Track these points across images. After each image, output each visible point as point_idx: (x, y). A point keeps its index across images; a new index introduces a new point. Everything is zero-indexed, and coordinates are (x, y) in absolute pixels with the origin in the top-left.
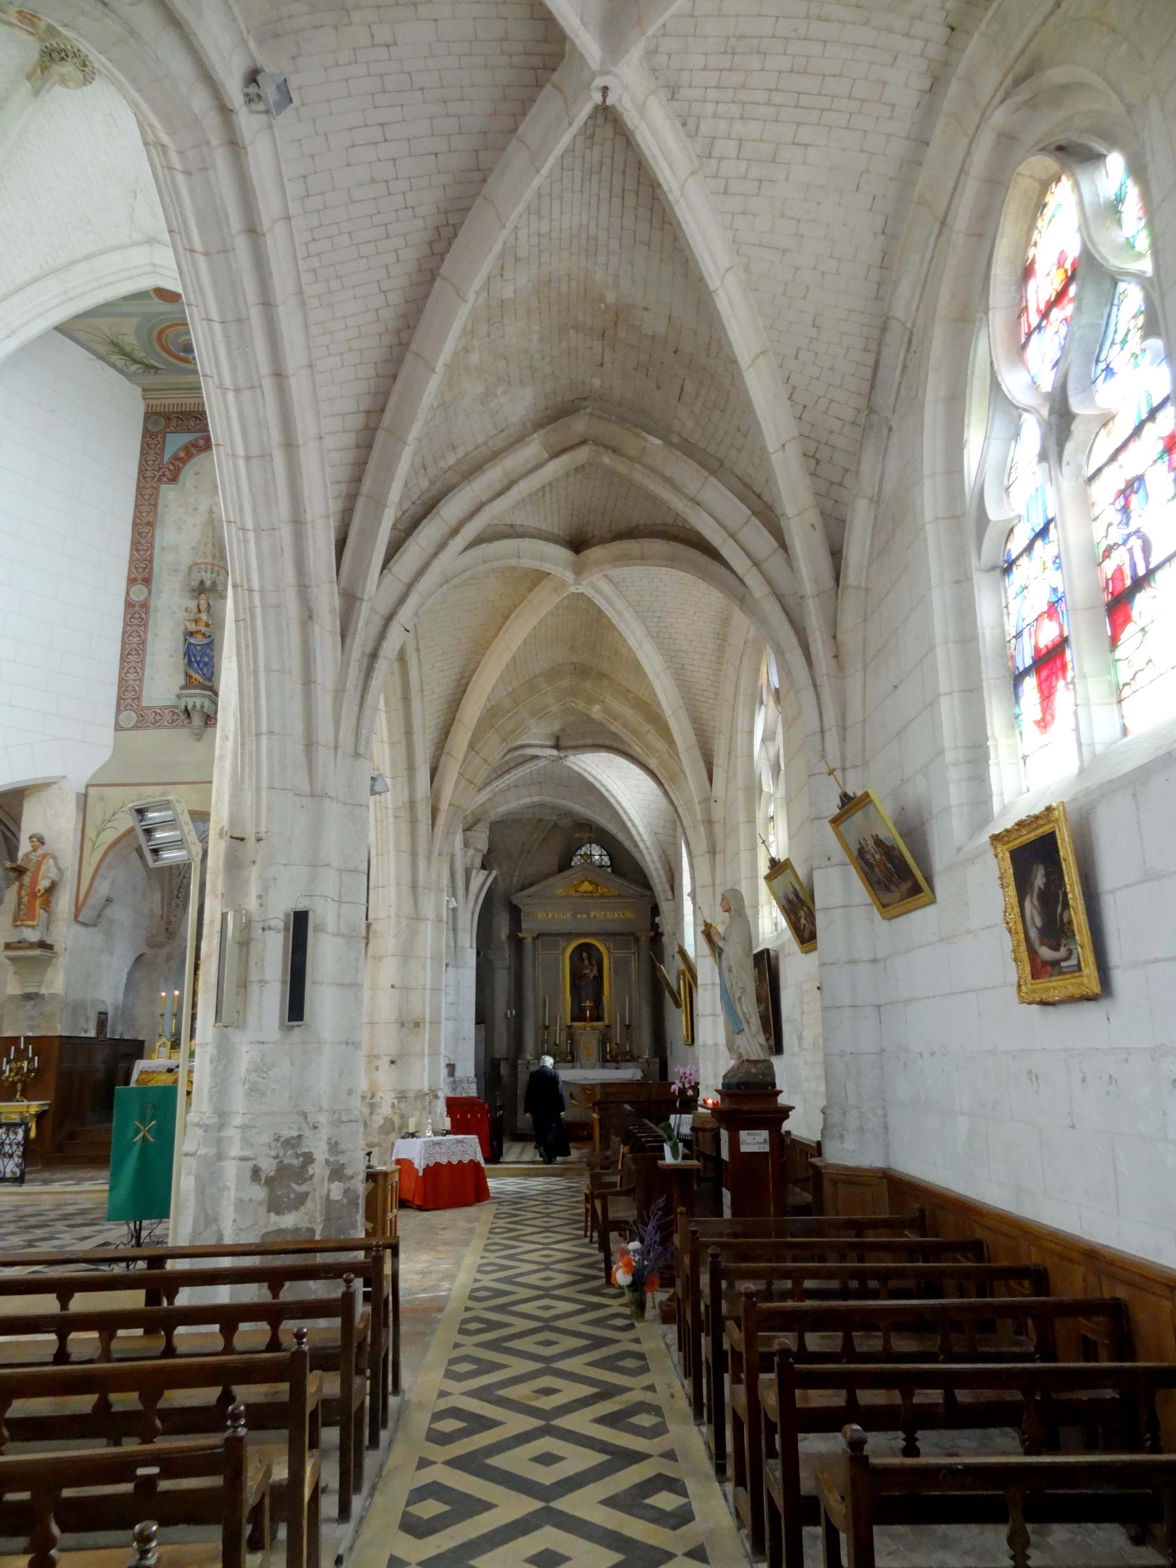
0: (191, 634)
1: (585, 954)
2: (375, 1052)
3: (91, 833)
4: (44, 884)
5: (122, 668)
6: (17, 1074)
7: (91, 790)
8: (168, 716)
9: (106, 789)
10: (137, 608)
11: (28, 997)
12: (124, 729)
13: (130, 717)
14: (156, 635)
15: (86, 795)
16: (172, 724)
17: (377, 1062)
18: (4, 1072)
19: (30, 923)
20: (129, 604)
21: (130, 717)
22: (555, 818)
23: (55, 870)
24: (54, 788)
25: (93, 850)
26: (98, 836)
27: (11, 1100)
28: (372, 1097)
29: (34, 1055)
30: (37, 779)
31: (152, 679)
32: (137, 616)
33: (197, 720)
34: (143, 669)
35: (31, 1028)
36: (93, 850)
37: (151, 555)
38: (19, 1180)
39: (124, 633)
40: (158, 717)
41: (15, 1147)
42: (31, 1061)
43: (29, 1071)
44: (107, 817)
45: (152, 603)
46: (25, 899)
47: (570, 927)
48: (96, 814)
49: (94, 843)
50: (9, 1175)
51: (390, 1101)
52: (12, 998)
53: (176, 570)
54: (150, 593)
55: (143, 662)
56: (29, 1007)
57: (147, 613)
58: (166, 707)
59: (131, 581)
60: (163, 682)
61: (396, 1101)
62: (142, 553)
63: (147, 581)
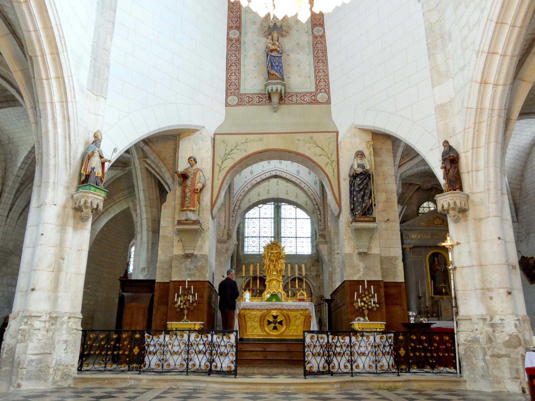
0: (272, 51)
1: (436, 259)
2: (488, 286)
3: (218, 161)
4: (199, 186)
5: (227, 73)
6: (185, 304)
7: (217, 136)
8: (256, 99)
9: (225, 136)
10: (234, 42)
11: (187, 256)
12: (231, 106)
13: (233, 99)
14: (246, 56)
15: (214, 139)
16: (259, 103)
17: (490, 294)
18: (177, 302)
19: (192, 209)
20: (229, 40)
21: (233, 99)
22: (421, 184)
23: (203, 178)
24: (197, 134)
25: (220, 171)
26: (222, 162)
27: (180, 321)
28: (491, 320)
29: (194, 292)
30: (190, 125)
31: (245, 79)
32: (234, 46)
33: (275, 99)
34: (239, 73)
35: (190, 276)
36: (220, 171)
37: (240, 15)
38: (233, 373)
39: (227, 54)
40: (250, 100)
41: (229, 349)
42: (194, 295)
43: (193, 302)
44: (227, 152)
45: (242, 39)
46: (188, 195)
47: (431, 243)
48: (221, 151)
49: (220, 167)
50: (225, 369)
51: (513, 323)
52: (177, 256)
53: (255, 22)
54: (240, 33)
55: (239, 70)
56: (188, 263)
57: (240, 44)
58: (255, 94)
59: (230, 28)
60: (252, 81)
61: (517, 322)
62: (235, 13)
63: (239, 28)
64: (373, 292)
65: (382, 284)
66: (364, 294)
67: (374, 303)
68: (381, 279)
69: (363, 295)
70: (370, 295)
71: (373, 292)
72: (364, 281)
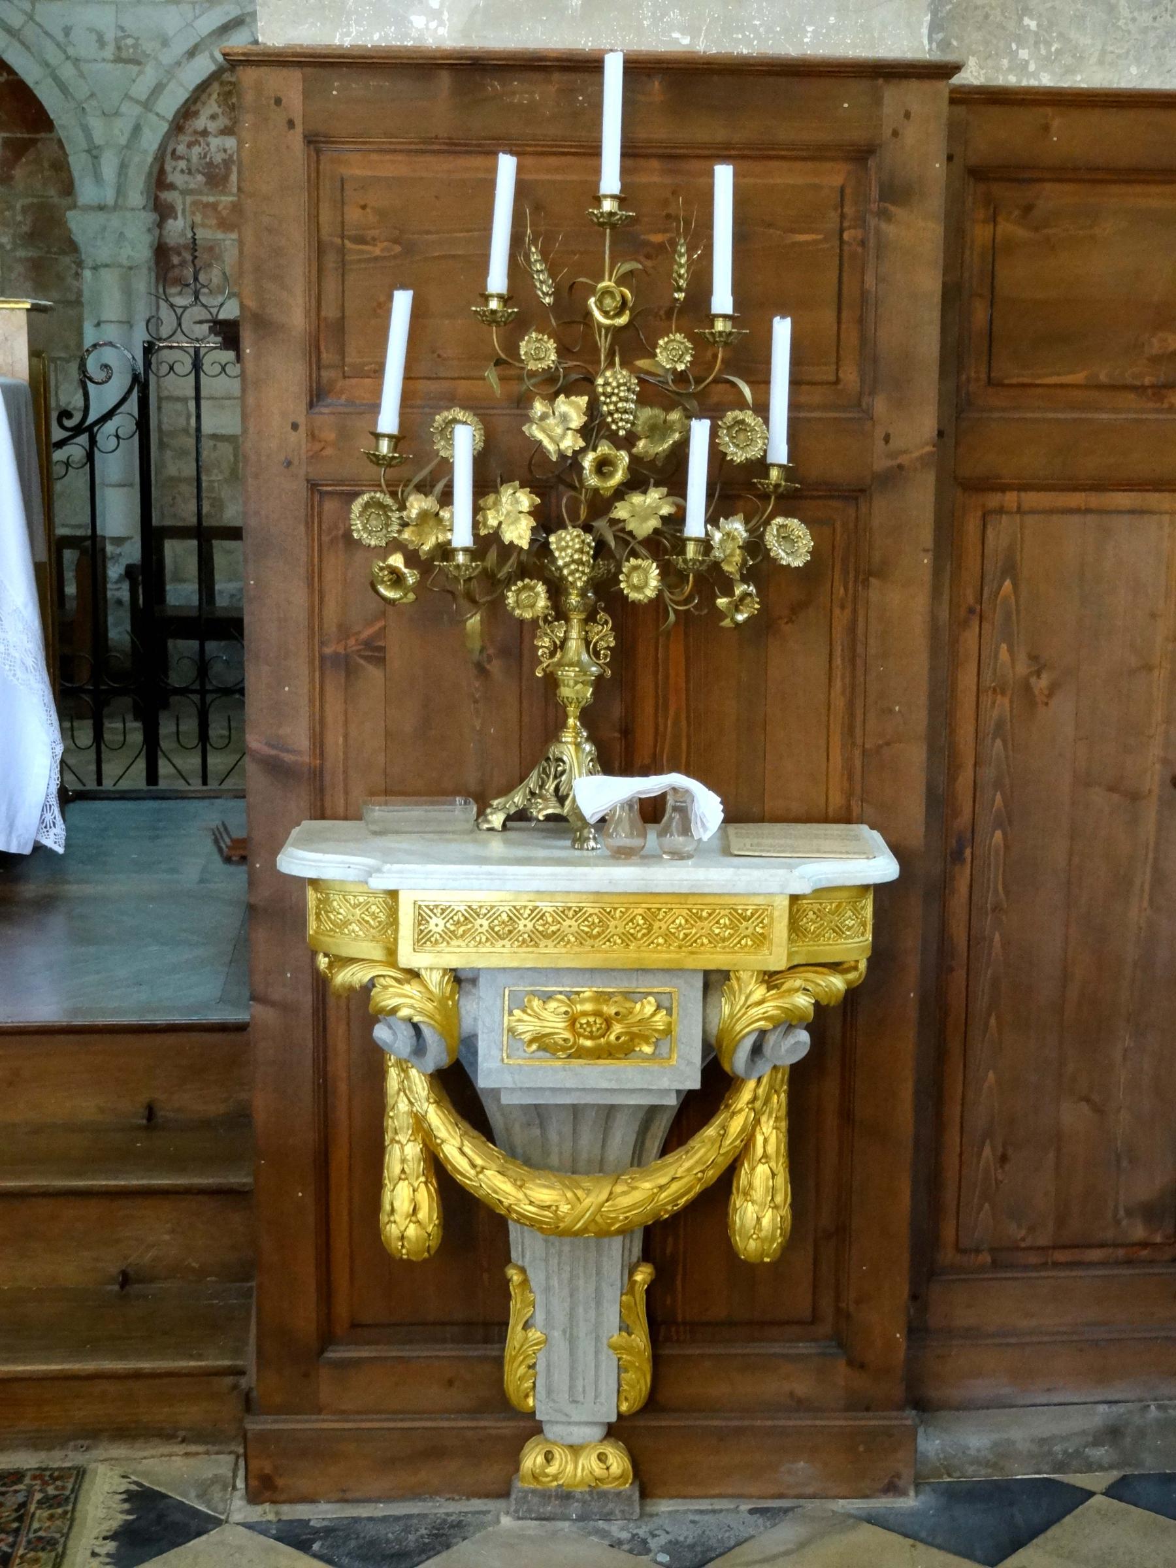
64: (722, 300)
65: (919, 140)
66: (569, 321)
67: (734, 487)
68: (907, 41)
69: (539, 351)
70: (672, 353)
71: (722, 300)
72: (589, 67)
